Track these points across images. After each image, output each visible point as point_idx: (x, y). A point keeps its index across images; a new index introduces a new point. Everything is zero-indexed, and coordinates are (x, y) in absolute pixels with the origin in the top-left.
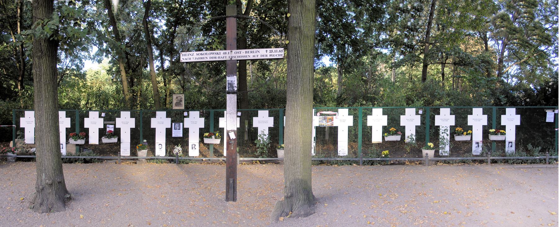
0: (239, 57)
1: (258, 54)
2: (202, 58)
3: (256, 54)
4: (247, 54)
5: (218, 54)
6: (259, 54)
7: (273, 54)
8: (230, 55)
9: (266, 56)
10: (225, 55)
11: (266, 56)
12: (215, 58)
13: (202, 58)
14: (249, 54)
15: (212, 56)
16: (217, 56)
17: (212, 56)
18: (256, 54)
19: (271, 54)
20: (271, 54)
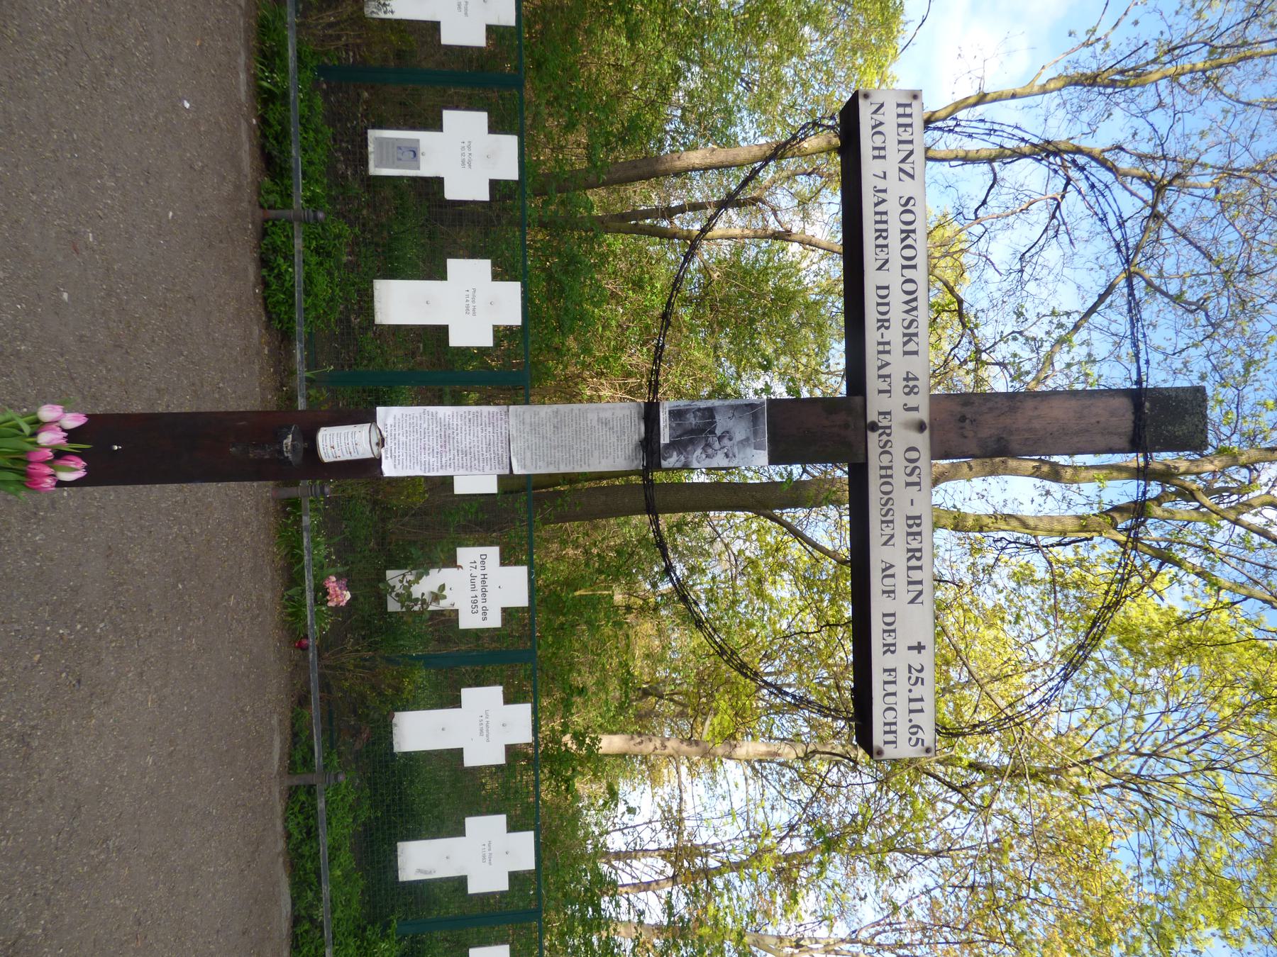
0: (887, 479)
1: (904, 593)
2: (881, 234)
3: (900, 582)
4: (900, 528)
5: (909, 337)
6: (899, 603)
7: (902, 686)
8: (900, 416)
9: (889, 648)
10: (898, 384)
11: (889, 648)
12: (883, 324)
13: (881, 234)
14: (900, 540)
15: (897, 299)
16: (895, 335)
17: (897, 299)
18: (900, 582)
19: (902, 675)
20: (902, 675)
